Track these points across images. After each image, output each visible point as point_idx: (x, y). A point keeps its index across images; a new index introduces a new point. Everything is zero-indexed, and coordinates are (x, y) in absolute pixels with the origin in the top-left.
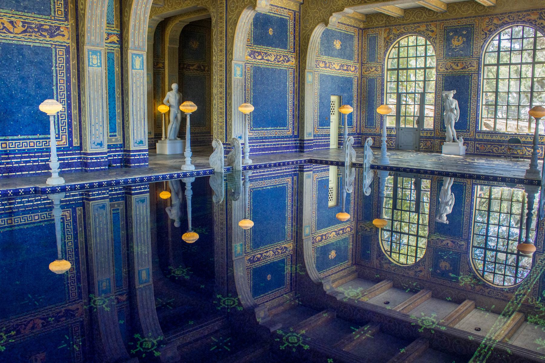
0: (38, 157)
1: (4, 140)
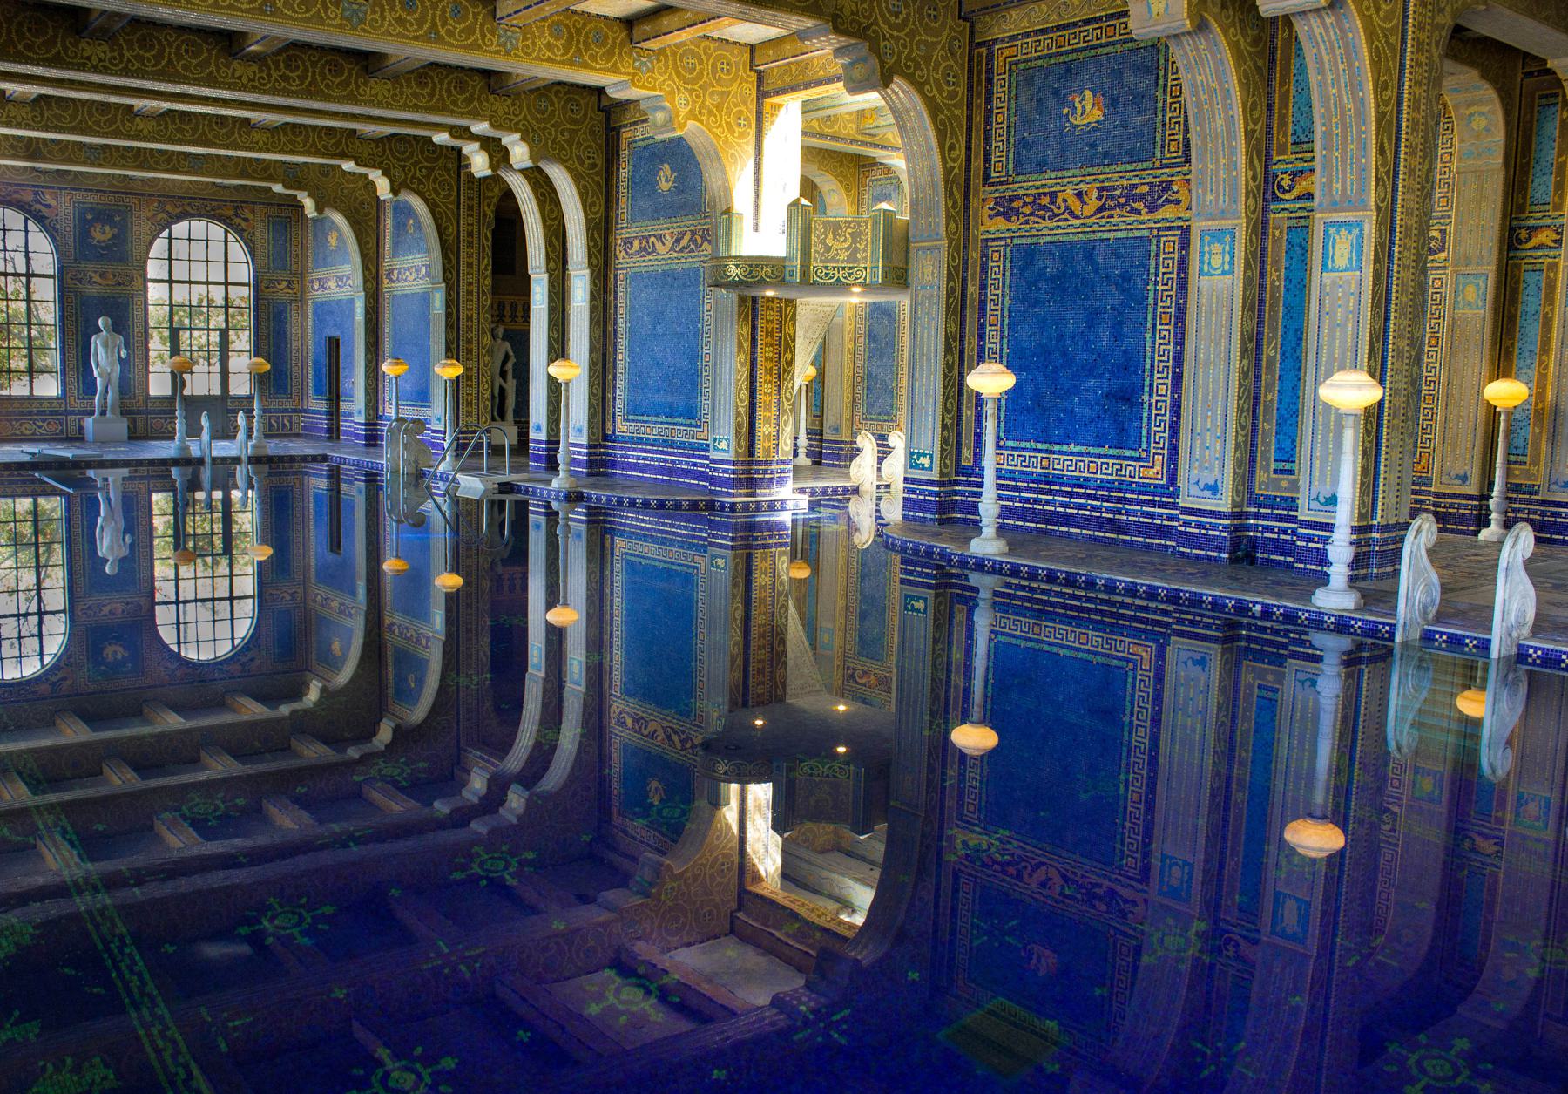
0: (1102, 498)
1: (1047, 451)
